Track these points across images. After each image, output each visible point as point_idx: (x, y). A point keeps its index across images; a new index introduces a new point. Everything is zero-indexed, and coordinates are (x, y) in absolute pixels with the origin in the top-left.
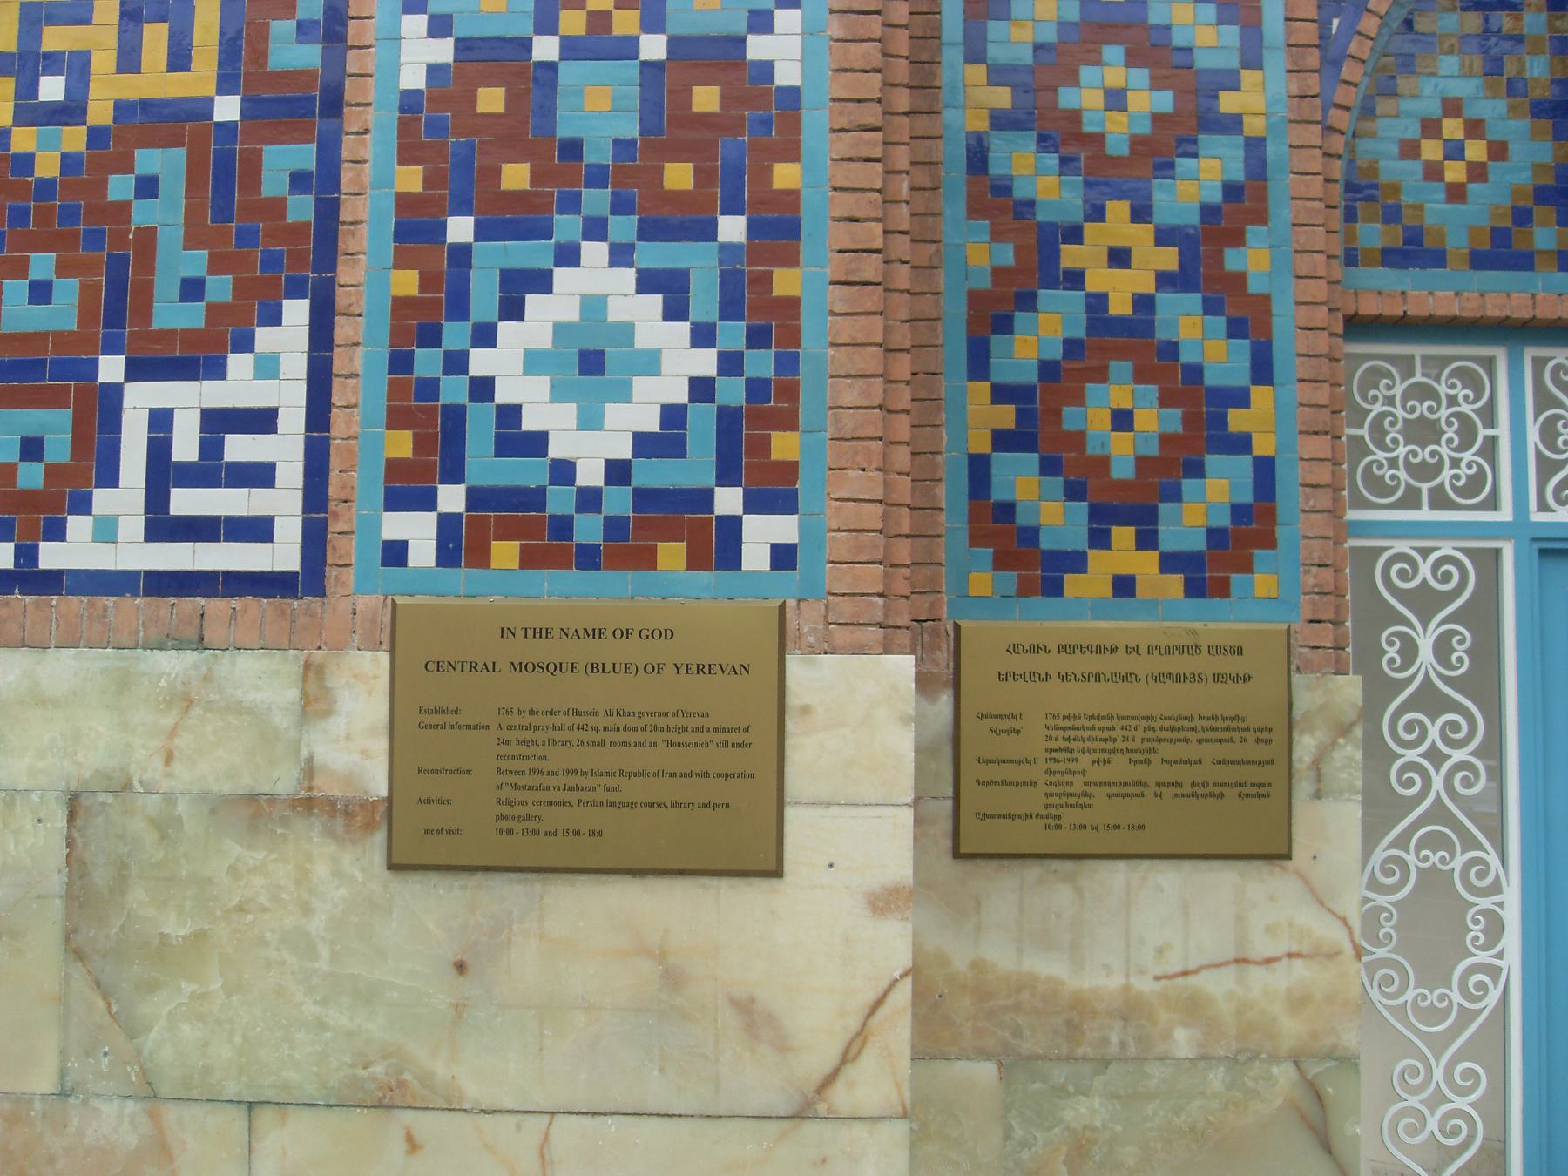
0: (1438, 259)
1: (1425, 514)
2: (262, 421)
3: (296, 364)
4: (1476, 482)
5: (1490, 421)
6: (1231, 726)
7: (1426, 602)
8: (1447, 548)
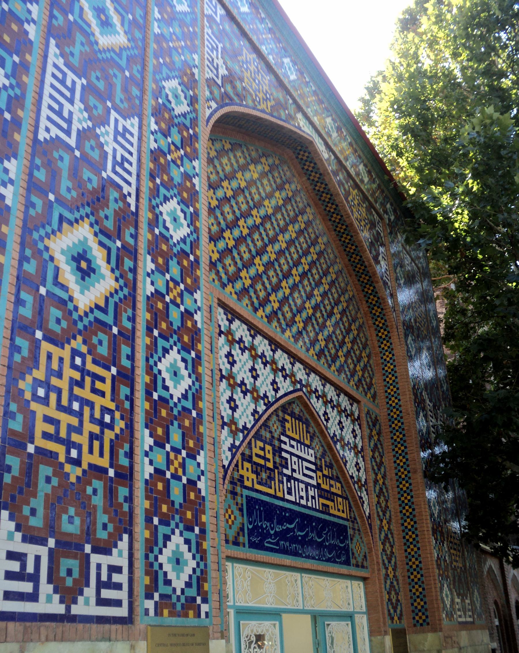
2: (118, 570)
3: (126, 554)
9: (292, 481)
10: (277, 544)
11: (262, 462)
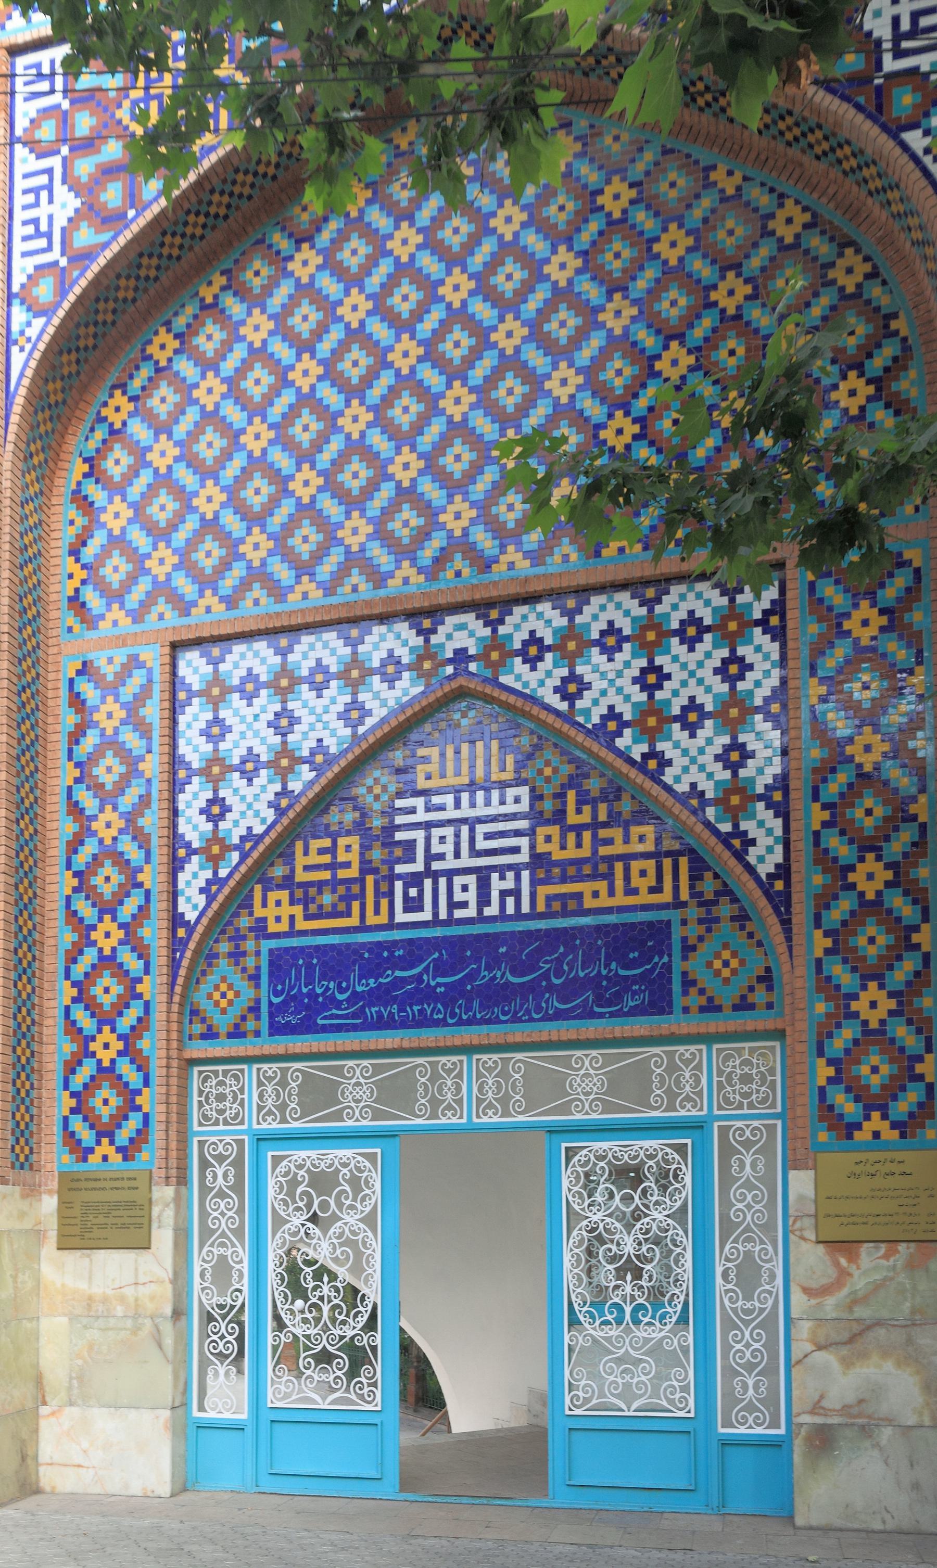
0: (215, 1036)
1: (221, 1127)
4: (237, 1114)
5: (242, 1093)
6: (131, 1205)
7: (221, 1159)
8: (228, 1139)
9: (428, 883)
10: (354, 1016)
11: (326, 875)
